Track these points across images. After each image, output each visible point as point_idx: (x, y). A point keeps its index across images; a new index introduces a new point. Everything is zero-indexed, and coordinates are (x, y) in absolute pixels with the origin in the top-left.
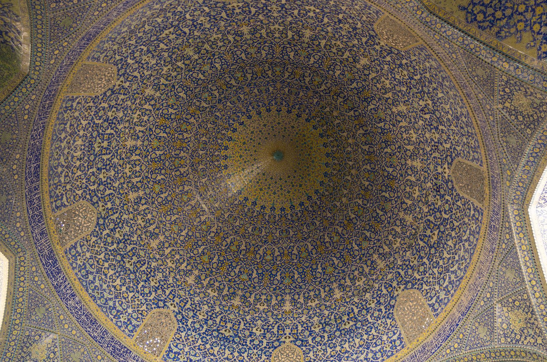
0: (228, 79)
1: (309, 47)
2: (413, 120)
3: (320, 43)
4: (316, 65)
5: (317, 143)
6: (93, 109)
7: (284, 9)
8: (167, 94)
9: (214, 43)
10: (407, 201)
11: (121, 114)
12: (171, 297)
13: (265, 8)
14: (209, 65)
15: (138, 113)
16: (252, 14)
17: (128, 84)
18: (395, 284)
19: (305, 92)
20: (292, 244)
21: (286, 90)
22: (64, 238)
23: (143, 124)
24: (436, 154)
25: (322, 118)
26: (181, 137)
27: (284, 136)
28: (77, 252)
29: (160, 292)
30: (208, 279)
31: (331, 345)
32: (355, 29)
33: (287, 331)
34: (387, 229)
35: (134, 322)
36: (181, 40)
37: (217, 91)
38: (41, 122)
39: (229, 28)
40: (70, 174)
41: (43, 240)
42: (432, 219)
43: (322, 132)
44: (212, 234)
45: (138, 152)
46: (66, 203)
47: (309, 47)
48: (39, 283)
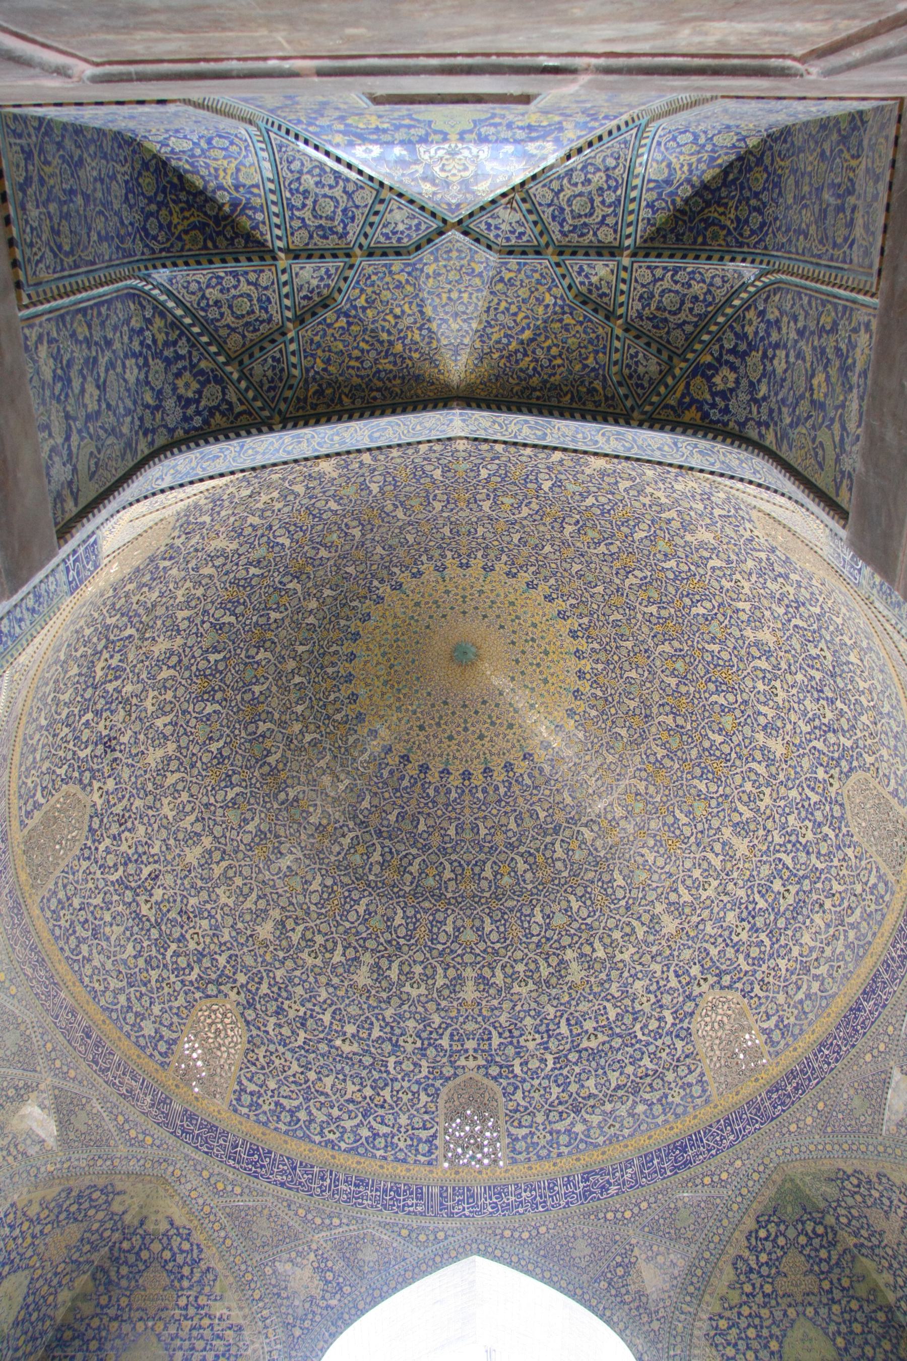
0: (529, 876)
1: (365, 940)
2: (171, 842)
3: (344, 954)
4: (355, 895)
5: (370, 697)
8: (644, 897)
10: (172, 672)
15: (704, 895)
16: (449, 1030)
19: (385, 823)
21: (422, 827)
23: (705, 865)
27: (445, 703)
29: (779, 569)
37: (556, 856)
39: (495, 1003)
45: (736, 818)
47: (365, 940)
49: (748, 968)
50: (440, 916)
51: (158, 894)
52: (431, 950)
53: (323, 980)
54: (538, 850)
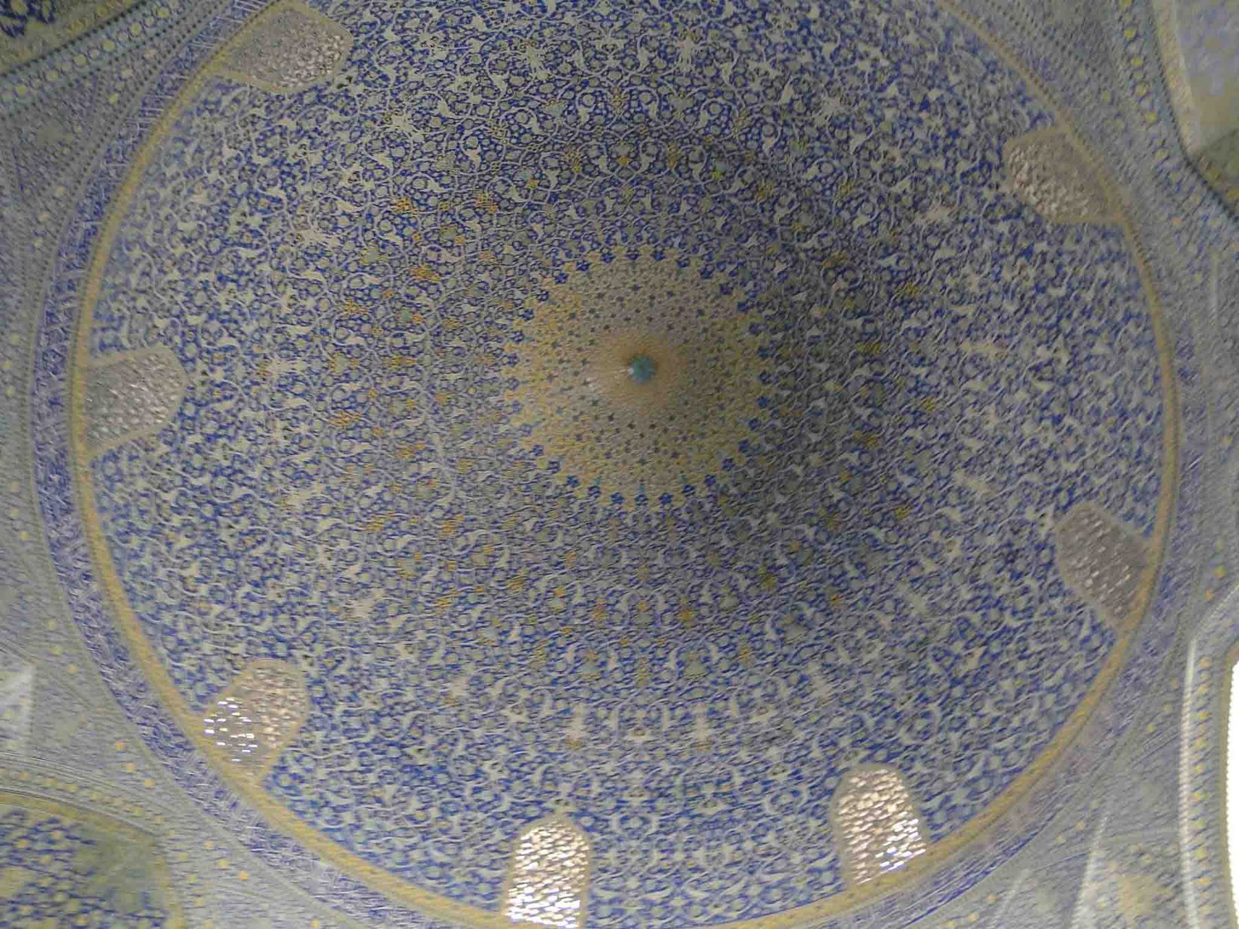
0: (593, 153)
3: (849, 138)
4: (818, 187)
5: (746, 368)
6: (261, 126)
7: (804, 32)
8: (438, 143)
9: (601, 56)
11: (315, 158)
12: (308, 637)
13: (759, 14)
14: (563, 106)
15: (356, 167)
16: (723, 17)
17: (362, 86)
18: (845, 742)
20: (619, 587)
21: (720, 221)
22: (95, 427)
24: (1034, 478)
25: (782, 314)
26: (432, 256)
28: (119, 471)
29: (283, 619)
30: (403, 617)
31: (664, 846)
32: (953, 134)
33: (565, 788)
34: (857, 613)
35: (212, 679)
36: (526, 24)
37: (557, 172)
38: (141, 120)
39: (650, 32)
40: (155, 271)
41: (50, 421)
42: (976, 618)
43: (767, 344)
44: (438, 513)
46: (125, 342)
48: (18, 525)
49: (281, 122)
50: (714, 130)
51: (1043, 353)
52: (734, 100)
53: (884, 127)
54: (579, 177)
